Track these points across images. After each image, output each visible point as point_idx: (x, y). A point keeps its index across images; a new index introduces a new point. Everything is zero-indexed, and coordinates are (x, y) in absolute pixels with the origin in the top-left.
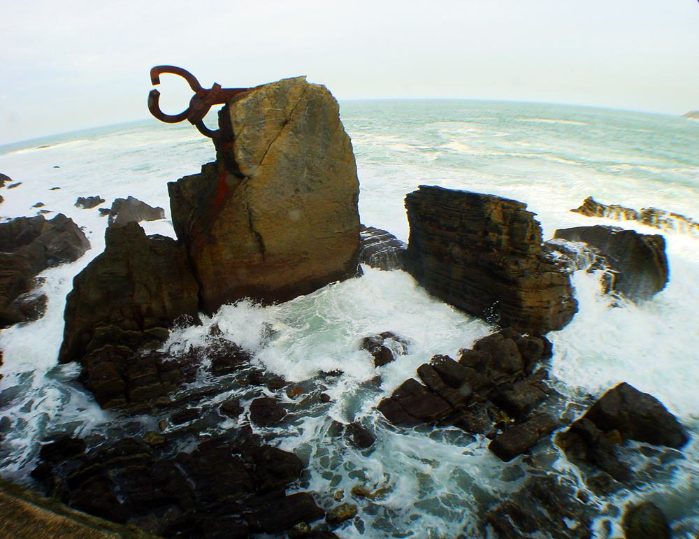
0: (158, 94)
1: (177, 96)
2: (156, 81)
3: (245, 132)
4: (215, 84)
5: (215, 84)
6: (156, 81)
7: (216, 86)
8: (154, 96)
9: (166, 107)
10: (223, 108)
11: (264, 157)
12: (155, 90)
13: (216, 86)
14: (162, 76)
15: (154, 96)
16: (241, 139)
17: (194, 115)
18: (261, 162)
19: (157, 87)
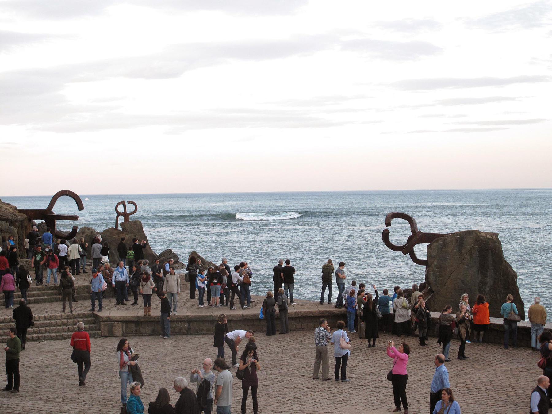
2: (388, 224)
3: (436, 263)
6: (388, 224)
12: (387, 230)
15: (385, 235)
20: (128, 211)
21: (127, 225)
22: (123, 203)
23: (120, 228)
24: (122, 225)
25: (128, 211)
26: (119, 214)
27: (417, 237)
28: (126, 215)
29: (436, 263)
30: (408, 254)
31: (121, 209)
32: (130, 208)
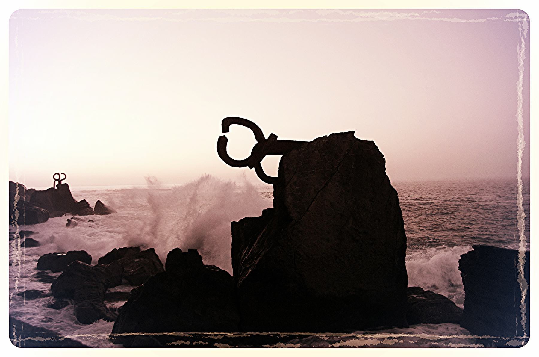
0: (227, 140)
1: (242, 143)
2: (225, 129)
3: (295, 179)
4: (272, 134)
5: (272, 134)
6: (225, 129)
7: (273, 137)
8: (222, 143)
9: (233, 152)
10: (281, 158)
11: (311, 204)
12: (224, 136)
13: (273, 137)
14: (232, 127)
15: (222, 143)
16: (291, 186)
17: (254, 161)
18: (308, 208)
19: (226, 134)
20: (61, 179)
21: (60, 186)
22: (58, 174)
23: (56, 188)
24: (57, 186)
25: (61, 179)
26: (56, 180)
27: (266, 145)
28: (60, 181)
29: (295, 179)
30: (253, 169)
31: (57, 177)
32: (62, 177)
